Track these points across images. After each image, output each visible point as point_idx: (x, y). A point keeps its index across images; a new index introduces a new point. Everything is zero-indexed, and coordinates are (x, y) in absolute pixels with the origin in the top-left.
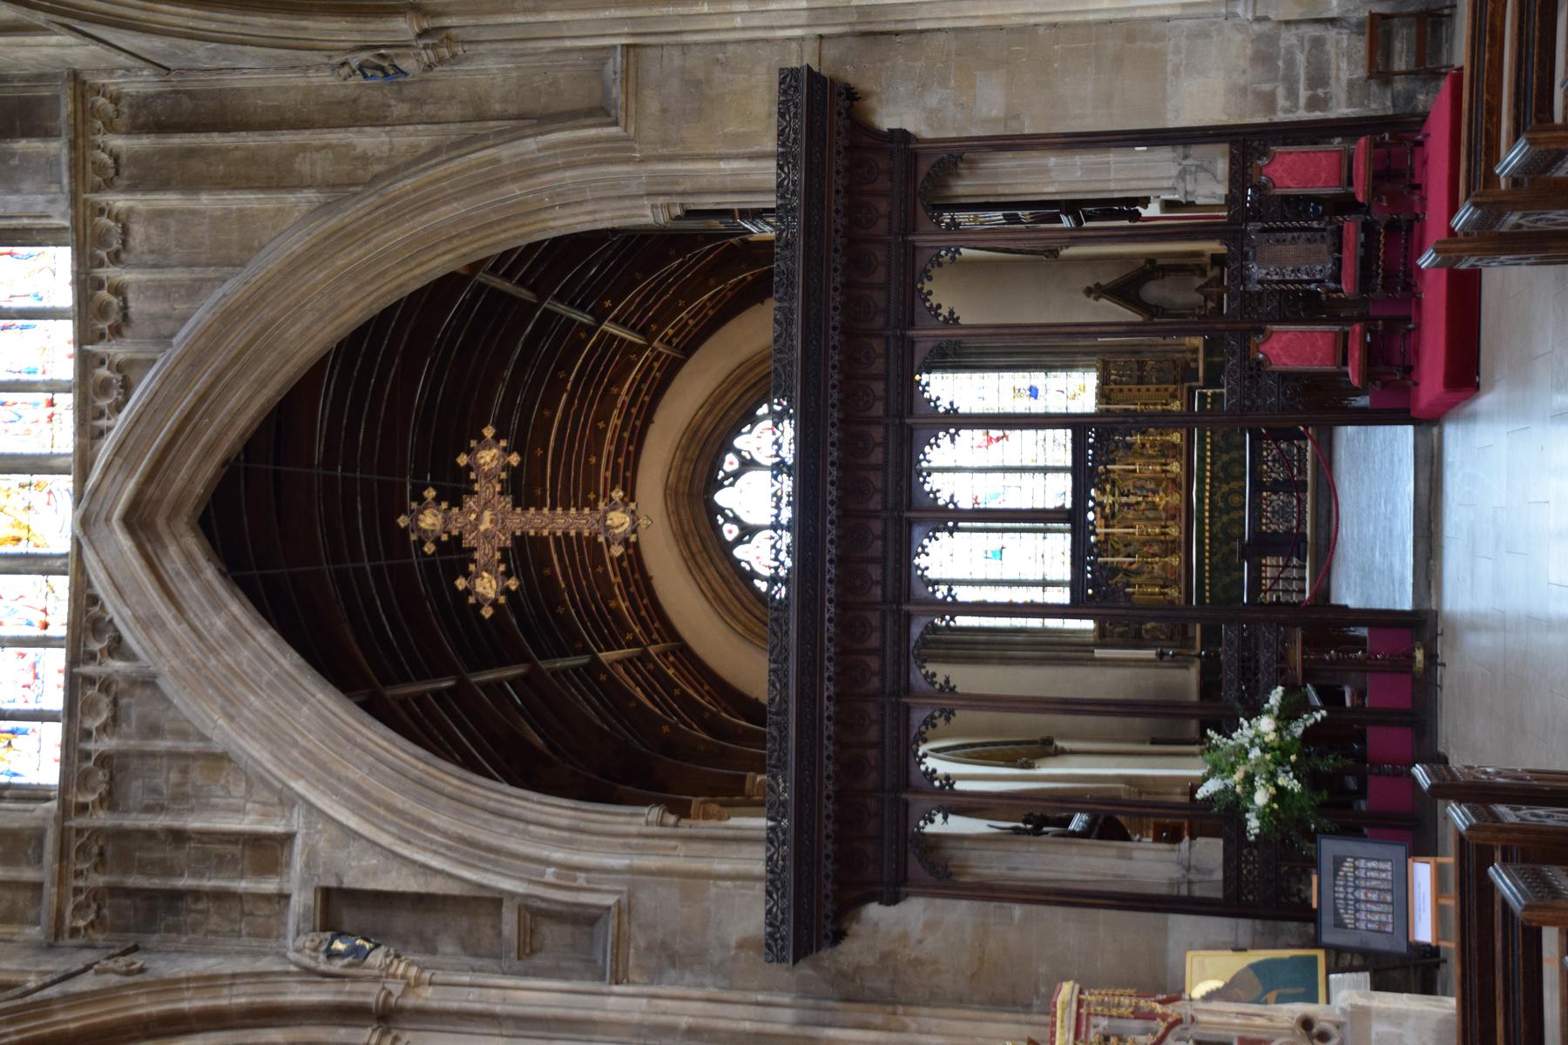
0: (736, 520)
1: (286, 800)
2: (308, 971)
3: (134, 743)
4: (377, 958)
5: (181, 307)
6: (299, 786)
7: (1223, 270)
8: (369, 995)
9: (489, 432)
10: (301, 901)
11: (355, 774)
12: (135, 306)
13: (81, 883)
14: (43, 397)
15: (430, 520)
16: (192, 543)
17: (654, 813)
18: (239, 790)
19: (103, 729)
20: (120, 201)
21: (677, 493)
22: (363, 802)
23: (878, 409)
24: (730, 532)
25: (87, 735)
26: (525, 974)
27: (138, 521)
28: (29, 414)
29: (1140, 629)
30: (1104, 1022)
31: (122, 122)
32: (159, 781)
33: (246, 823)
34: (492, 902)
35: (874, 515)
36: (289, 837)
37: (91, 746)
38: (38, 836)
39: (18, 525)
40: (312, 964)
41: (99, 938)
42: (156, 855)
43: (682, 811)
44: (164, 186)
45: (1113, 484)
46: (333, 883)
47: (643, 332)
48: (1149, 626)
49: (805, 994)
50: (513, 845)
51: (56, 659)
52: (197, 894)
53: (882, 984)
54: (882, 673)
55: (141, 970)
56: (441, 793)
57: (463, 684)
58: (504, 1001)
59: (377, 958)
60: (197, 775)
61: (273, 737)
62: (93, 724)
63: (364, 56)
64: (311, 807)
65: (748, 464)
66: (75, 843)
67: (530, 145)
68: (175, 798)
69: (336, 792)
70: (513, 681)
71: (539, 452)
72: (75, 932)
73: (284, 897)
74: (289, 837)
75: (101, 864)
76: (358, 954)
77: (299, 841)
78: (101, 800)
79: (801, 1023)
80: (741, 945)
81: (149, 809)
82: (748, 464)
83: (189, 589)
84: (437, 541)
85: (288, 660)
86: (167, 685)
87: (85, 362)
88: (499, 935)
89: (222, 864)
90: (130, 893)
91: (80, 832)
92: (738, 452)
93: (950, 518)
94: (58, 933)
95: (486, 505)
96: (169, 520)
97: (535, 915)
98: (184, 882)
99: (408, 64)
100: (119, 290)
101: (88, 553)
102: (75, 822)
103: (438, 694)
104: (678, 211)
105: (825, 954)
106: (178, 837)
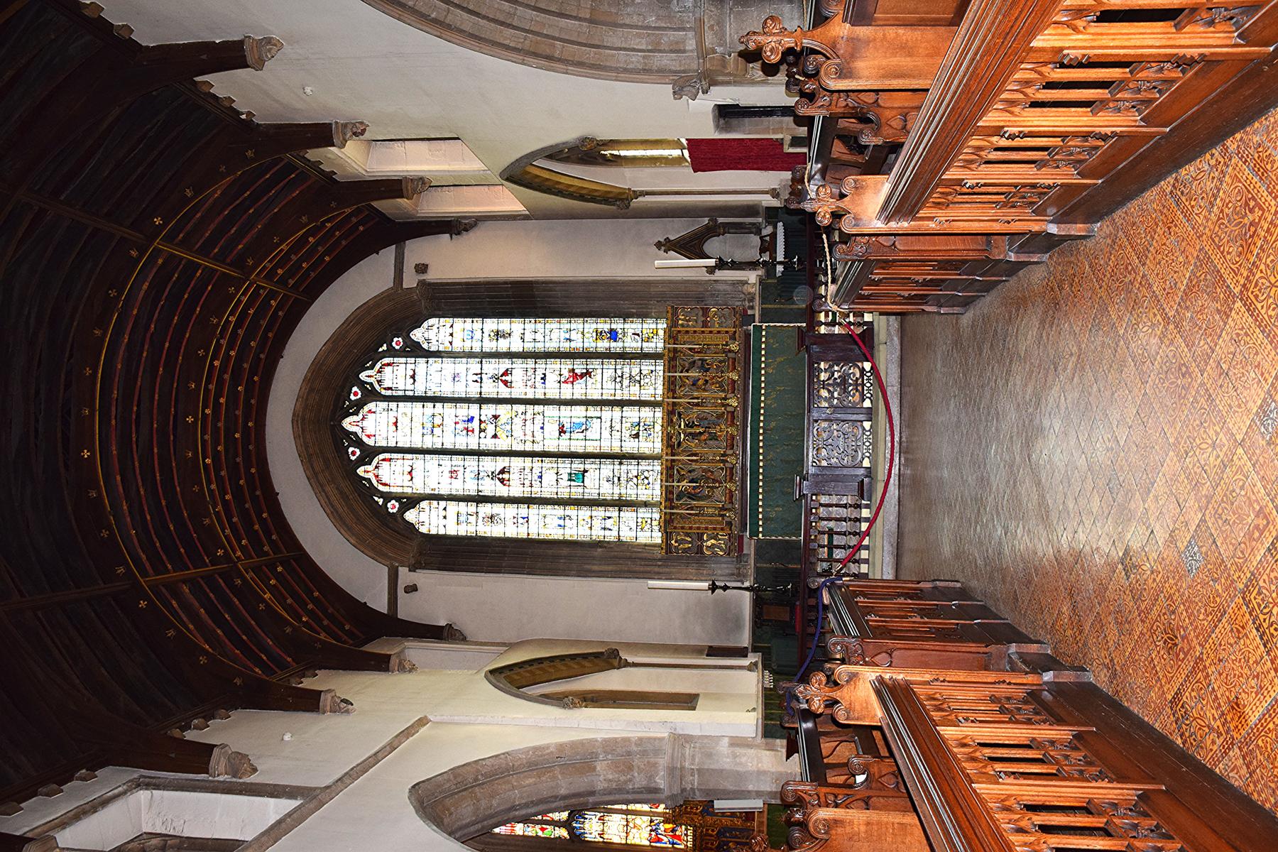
0: (359, 443)
7: (775, 227)
21: (303, 419)
24: (354, 453)
29: (702, 546)
45: (680, 415)
47: (239, 263)
48: (709, 543)
71: (88, 371)
82: (371, 394)
92: (362, 384)
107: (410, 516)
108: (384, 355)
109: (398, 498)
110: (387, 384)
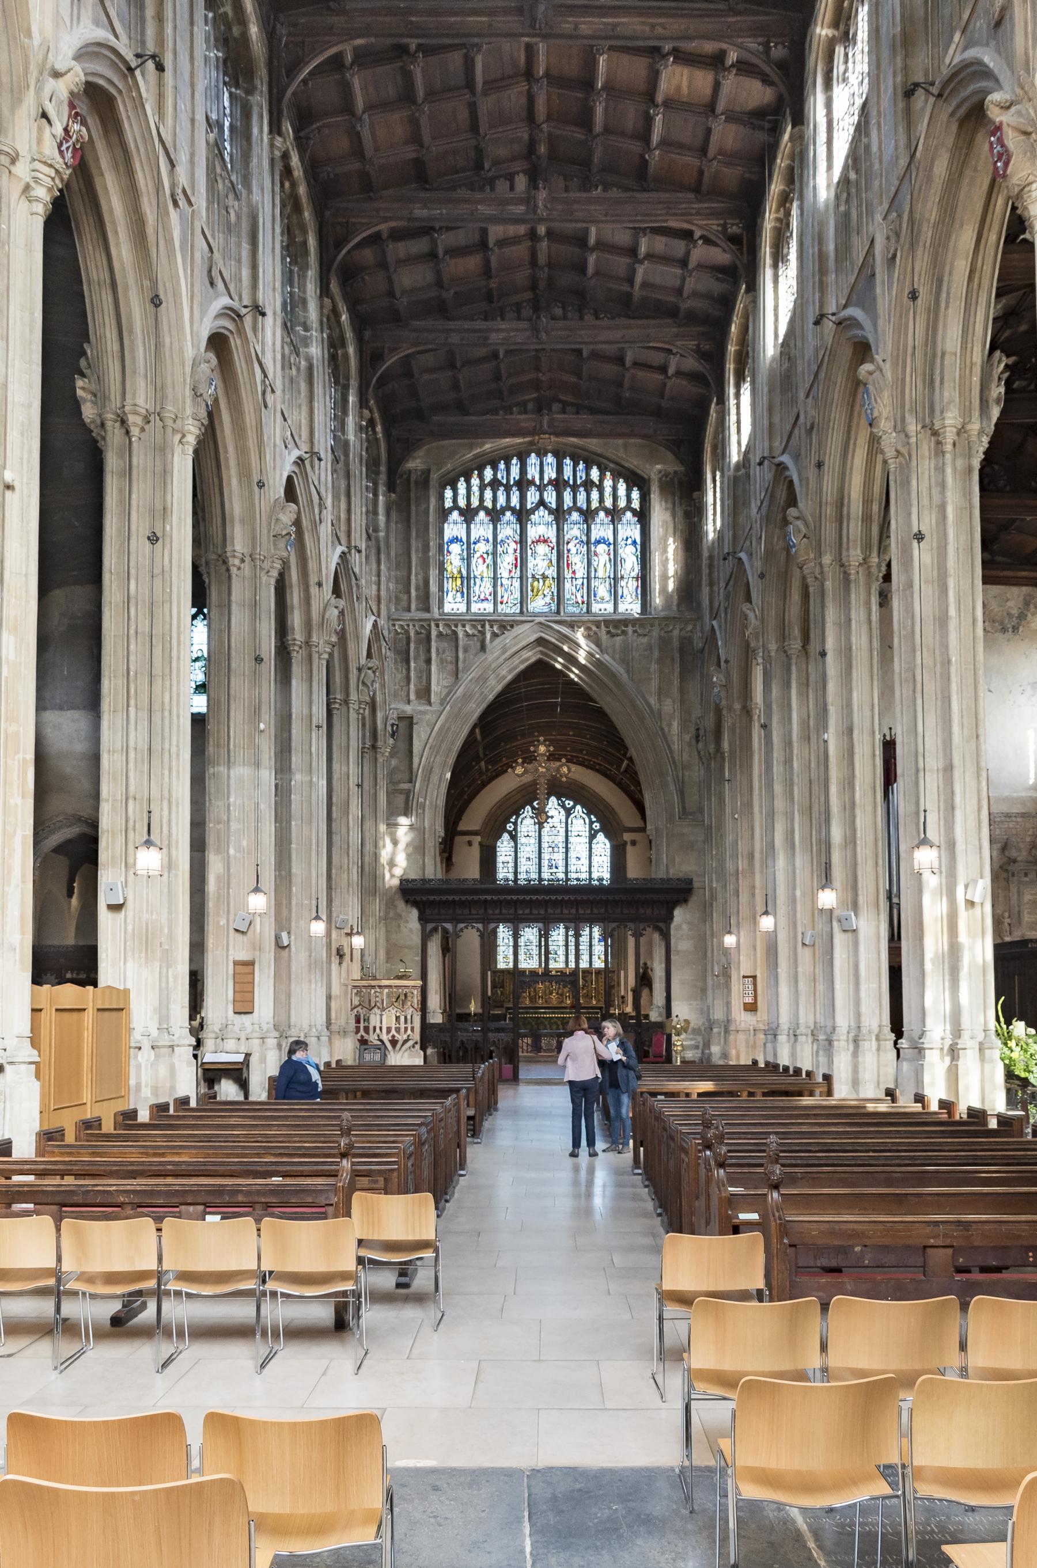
2: (387, 719)
3: (461, 643)
4: (391, 741)
5: (617, 656)
6: (448, 708)
10: (408, 709)
12: (618, 639)
13: (411, 627)
14: (585, 599)
15: (542, 749)
16: (533, 659)
17: (442, 834)
19: (466, 631)
20: (655, 633)
23: (581, 911)
25: (464, 626)
27: (540, 641)
28: (579, 595)
31: (683, 633)
32: (447, 653)
35: (546, 910)
36: (430, 704)
37: (460, 628)
38: (427, 609)
39: (538, 591)
41: (392, 635)
42: (421, 653)
43: (441, 843)
44: (661, 650)
51: (489, 607)
52: (408, 669)
53: (391, 914)
54: (494, 914)
60: (451, 667)
61: (467, 697)
62: (468, 628)
65: (568, 812)
66: (425, 624)
67: (672, 787)
72: (394, 625)
73: (409, 702)
74: (430, 704)
75: (417, 633)
77: (429, 708)
81: (437, 650)
82: (568, 812)
83: (516, 661)
84: (535, 752)
85: (491, 697)
86: (482, 657)
87: (598, 624)
91: (429, 625)
92: (574, 807)
93: (545, 935)
94: (393, 620)
98: (412, 665)
99: (700, 745)
100: (624, 633)
101: (527, 626)
102: (433, 624)
106: (428, 661)
107: (506, 836)
108: (590, 819)
109: (515, 829)
110: (574, 820)
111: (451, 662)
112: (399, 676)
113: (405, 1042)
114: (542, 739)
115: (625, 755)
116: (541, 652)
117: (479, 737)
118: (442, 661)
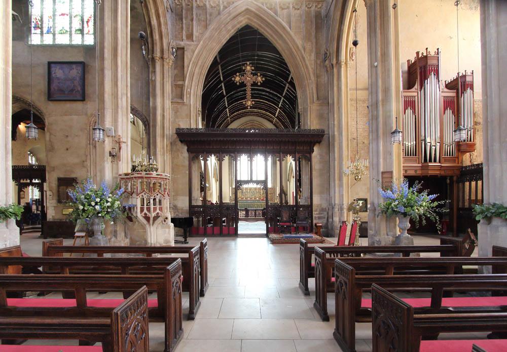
1: (199, 41)
3: (208, 11)
6: (201, 42)
8: (166, 56)
9: (264, 79)
10: (182, 44)
11: (204, 54)
15: (248, 68)
16: (243, 24)
18: (201, 32)
22: (199, 55)
26: (172, 85)
30: (163, 183)
33: (195, 33)
34: (184, 80)
36: (193, 41)
40: (171, 44)
46: (185, 49)
49: (172, 136)
50: (193, 83)
52: (182, 24)
55: (168, 11)
56: (202, 70)
57: (222, 82)
58: (166, 82)
59: (172, 57)
61: (210, 38)
63: (329, 54)
64: (198, 45)
68: (199, 19)
69: (201, 49)
70: (223, 92)
76: (173, 54)
78: (198, 5)
79: (166, 135)
80: (179, 125)
81: (197, 14)
85: (224, 41)
88: (178, 81)
89: (188, 29)
90: (182, 11)
95: (252, 79)
96: (248, 18)
97: (182, 87)
103: (220, 77)
104: (300, 113)
105: (178, 139)
106: (192, 20)
111: (204, 21)
112: (178, 27)
113: (156, 218)
114: (248, 63)
115: (286, 79)
116: (248, 18)
117: (219, 60)
118: (199, 20)
